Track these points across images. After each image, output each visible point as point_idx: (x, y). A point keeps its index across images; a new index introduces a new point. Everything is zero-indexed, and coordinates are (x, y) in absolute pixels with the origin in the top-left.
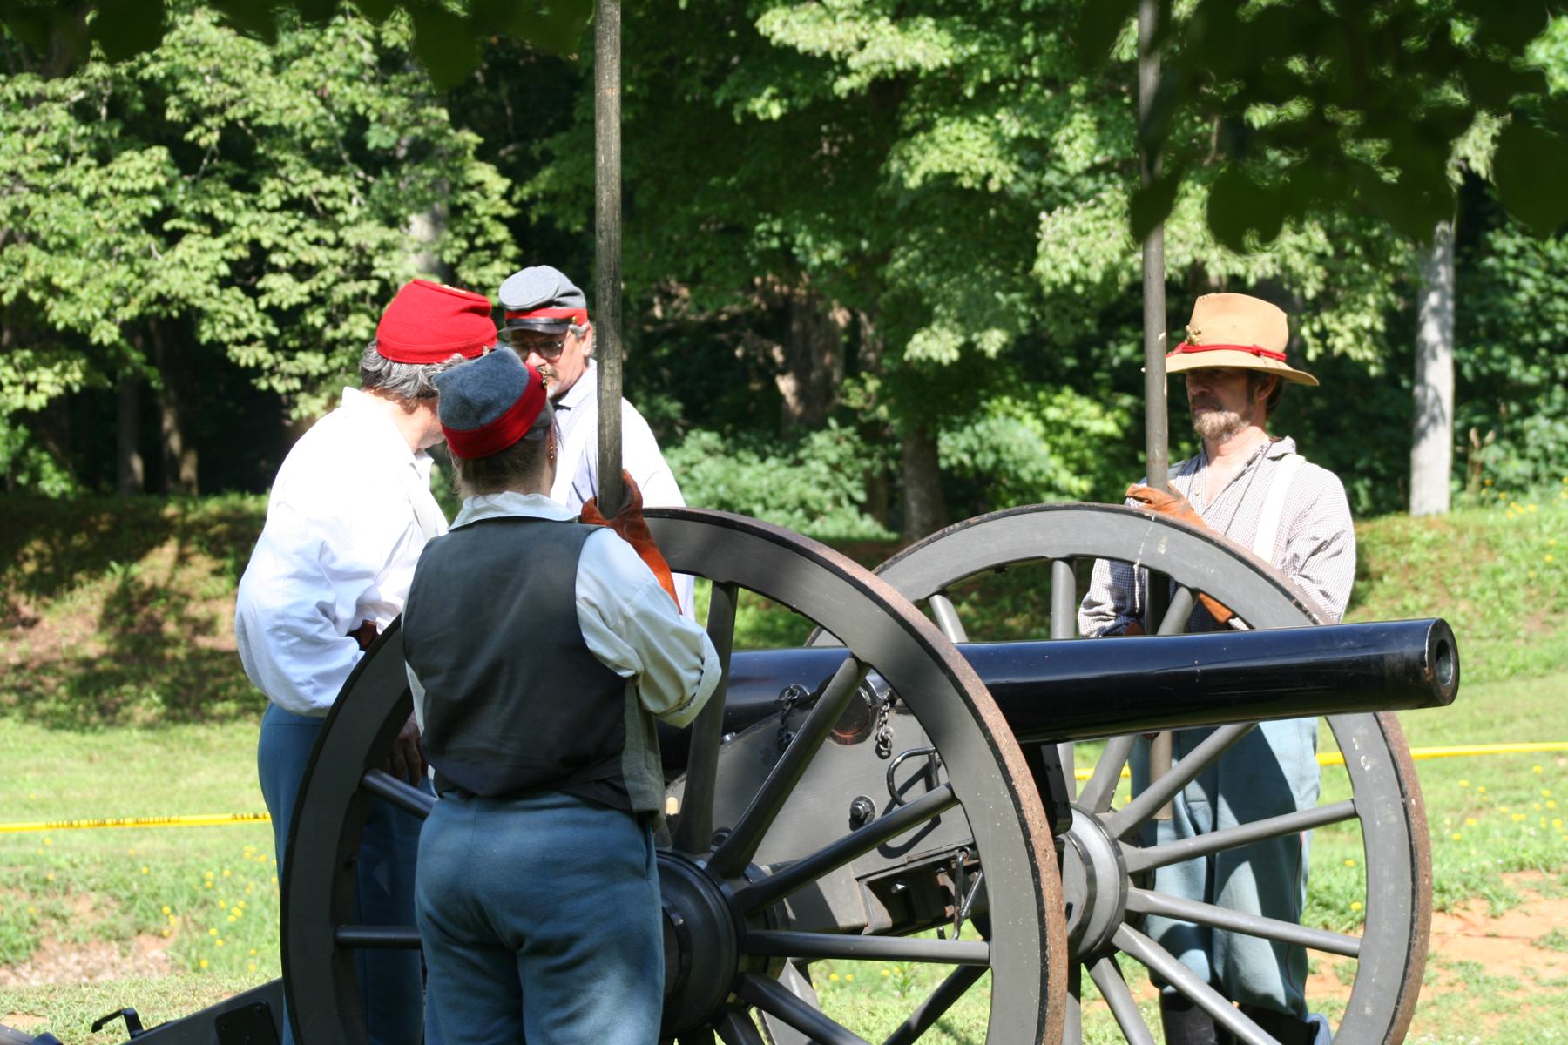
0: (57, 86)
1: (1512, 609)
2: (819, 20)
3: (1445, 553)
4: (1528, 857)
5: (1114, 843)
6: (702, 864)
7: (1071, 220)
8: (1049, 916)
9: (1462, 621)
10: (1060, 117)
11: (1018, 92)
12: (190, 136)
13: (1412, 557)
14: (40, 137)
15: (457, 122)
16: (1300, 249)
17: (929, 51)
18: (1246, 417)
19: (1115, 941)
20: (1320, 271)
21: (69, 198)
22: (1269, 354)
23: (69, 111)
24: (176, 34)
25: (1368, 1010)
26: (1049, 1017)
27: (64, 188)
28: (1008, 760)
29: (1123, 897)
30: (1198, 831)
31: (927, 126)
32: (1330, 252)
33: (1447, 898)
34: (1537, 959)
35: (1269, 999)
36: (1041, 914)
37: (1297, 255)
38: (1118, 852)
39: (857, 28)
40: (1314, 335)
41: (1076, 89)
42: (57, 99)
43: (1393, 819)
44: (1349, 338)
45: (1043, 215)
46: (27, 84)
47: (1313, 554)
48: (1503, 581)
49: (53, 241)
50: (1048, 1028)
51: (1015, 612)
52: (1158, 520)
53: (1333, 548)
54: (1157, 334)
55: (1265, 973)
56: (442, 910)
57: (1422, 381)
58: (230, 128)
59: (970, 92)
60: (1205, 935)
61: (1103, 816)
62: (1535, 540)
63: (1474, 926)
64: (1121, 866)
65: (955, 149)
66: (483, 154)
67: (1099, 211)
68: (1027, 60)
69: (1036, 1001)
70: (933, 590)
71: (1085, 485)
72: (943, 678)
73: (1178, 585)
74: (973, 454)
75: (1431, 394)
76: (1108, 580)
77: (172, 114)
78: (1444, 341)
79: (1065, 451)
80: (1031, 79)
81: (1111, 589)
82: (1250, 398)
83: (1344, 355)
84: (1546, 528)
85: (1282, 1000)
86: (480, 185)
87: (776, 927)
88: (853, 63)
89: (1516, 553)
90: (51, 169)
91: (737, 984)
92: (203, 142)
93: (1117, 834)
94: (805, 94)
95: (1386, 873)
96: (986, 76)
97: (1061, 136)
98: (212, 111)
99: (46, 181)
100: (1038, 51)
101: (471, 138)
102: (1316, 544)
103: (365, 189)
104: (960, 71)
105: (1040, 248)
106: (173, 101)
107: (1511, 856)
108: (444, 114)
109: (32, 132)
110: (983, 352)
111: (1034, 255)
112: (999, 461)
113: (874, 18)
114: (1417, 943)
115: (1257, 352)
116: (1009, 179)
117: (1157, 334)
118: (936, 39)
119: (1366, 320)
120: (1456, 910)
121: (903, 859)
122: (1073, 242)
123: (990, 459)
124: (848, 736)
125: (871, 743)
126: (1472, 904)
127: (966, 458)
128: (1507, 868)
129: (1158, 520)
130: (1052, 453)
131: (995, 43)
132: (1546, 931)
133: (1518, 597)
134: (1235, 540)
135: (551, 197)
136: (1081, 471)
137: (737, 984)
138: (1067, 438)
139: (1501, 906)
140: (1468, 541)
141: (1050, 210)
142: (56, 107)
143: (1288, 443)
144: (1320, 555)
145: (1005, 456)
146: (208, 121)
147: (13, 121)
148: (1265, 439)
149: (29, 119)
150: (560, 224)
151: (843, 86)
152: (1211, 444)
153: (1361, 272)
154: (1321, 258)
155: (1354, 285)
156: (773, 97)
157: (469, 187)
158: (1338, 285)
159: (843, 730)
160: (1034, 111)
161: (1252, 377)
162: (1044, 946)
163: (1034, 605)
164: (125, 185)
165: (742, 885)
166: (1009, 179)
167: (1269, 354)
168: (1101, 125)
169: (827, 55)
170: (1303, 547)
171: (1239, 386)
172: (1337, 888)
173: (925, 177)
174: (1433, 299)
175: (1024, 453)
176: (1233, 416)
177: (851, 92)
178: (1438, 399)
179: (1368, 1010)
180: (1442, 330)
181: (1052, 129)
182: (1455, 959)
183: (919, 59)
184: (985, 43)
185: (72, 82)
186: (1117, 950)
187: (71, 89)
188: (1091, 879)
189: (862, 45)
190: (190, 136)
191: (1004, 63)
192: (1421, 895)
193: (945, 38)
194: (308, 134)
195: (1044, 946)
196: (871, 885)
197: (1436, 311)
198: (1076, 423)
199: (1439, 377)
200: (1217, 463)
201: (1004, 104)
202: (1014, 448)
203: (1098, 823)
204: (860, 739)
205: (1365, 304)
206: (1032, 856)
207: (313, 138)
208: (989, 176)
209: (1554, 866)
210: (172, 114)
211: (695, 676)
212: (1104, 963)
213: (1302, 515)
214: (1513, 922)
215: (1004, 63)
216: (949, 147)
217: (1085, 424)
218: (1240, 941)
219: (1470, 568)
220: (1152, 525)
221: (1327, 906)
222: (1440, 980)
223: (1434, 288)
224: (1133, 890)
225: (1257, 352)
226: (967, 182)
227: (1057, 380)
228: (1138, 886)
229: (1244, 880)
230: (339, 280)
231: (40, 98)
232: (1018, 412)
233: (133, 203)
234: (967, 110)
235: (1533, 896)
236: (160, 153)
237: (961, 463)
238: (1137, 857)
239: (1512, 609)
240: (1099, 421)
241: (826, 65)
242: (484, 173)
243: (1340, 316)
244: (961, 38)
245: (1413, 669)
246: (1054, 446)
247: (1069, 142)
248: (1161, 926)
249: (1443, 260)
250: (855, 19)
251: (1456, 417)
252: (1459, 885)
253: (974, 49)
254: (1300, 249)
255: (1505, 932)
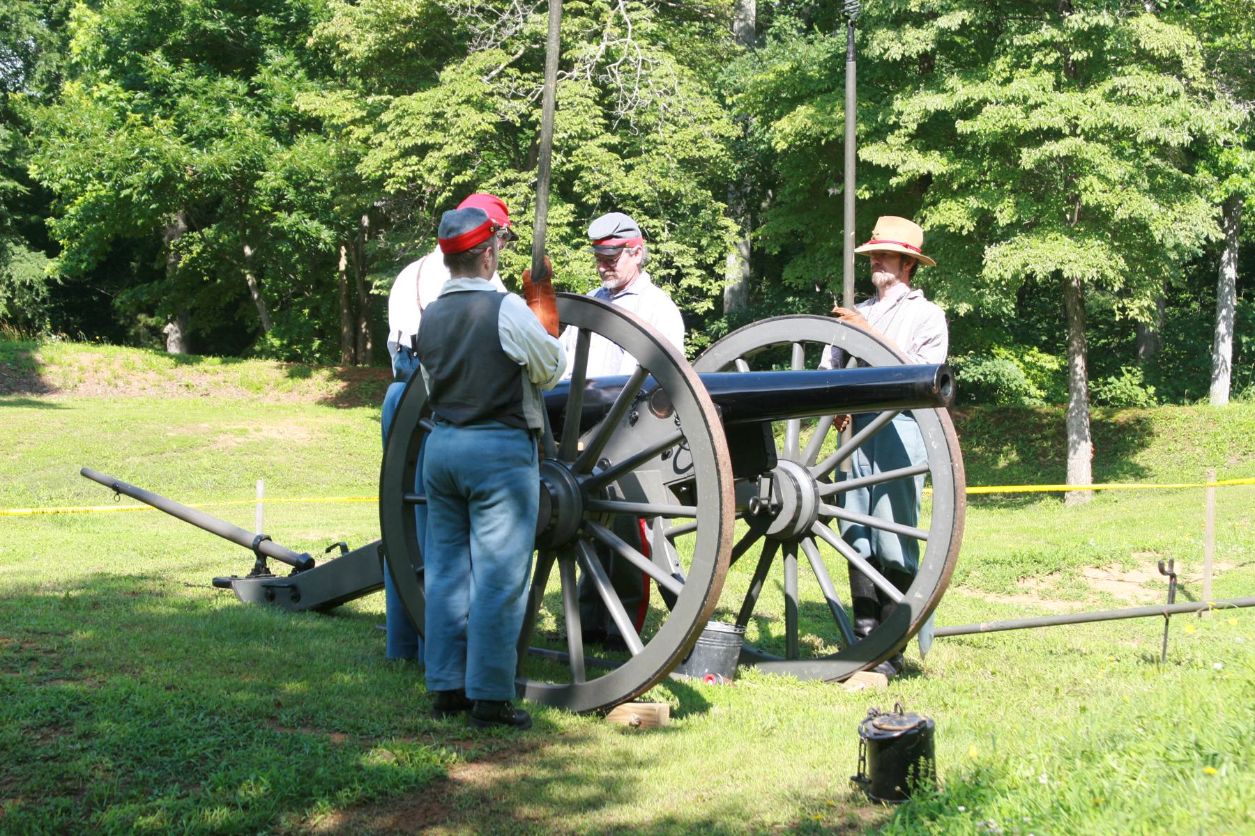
0: (524, 175)
1: (1222, 452)
2: (884, 150)
3: (1191, 424)
4: (1147, 546)
5: (813, 481)
6: (570, 467)
7: (998, 250)
8: (724, 495)
9: (1197, 457)
10: (997, 200)
11: (979, 188)
12: (584, 199)
13: (1174, 426)
14: (515, 198)
15: (716, 197)
16: (1111, 267)
17: (937, 167)
18: (898, 277)
19: (813, 529)
20: (1121, 278)
21: (528, 228)
22: (912, 248)
23: (529, 187)
24: (580, 150)
25: (930, 567)
26: (722, 544)
27: (526, 223)
28: (708, 418)
29: (816, 507)
30: (863, 475)
31: (935, 203)
32: (1127, 269)
33: (1100, 562)
34: (1141, 593)
35: (896, 563)
36: (720, 493)
37: (1110, 270)
38: (815, 486)
39: (902, 154)
40: (1119, 309)
41: (1008, 187)
42: (525, 181)
43: (947, 473)
44: (1137, 311)
45: (986, 247)
46: (511, 174)
47: (925, 344)
48: (1219, 439)
49: (520, 247)
50: (721, 549)
51: (978, 445)
52: (843, 324)
53: (936, 342)
54: (850, 233)
55: (894, 551)
56: (434, 478)
57: (1217, 352)
58: (605, 196)
59: (955, 187)
60: (868, 531)
61: (810, 468)
62: (1237, 419)
63: (1113, 576)
64: (816, 493)
65: (947, 214)
66: (727, 214)
67: (1013, 246)
68: (985, 174)
69: (717, 536)
70: (738, 355)
71: (1043, 394)
72: (680, 376)
73: (850, 356)
74: (985, 376)
75: (1221, 359)
76: (830, 357)
77: (576, 189)
78: (1229, 333)
79: (1034, 378)
80: (986, 182)
81: (831, 361)
82: (901, 269)
83: (1134, 321)
84: (1243, 414)
85: (903, 565)
86: (726, 228)
87: (606, 498)
88: (900, 170)
89: (1227, 426)
90: (521, 214)
91: (583, 525)
92: (590, 202)
93: (815, 477)
94: (881, 188)
95: (942, 499)
96: (963, 181)
97: (998, 208)
98: (597, 187)
99: (516, 219)
100: (989, 169)
101: (722, 205)
102: (925, 340)
103: (672, 229)
104: (952, 176)
105: (983, 263)
106: (577, 182)
107: (1140, 545)
108: (710, 193)
109: (512, 196)
110: (958, 313)
111: (981, 267)
112: (998, 379)
113: (910, 149)
114: (955, 534)
115: (906, 246)
116: (972, 229)
117: (850, 233)
118: (940, 161)
119: (1145, 303)
120: (1105, 568)
121: (685, 475)
122: (999, 260)
123: (994, 379)
124: (663, 414)
125: (673, 418)
126: (1114, 565)
127: (982, 378)
128: (1135, 550)
129: (843, 324)
130: (1026, 378)
131: (970, 164)
132: (1149, 580)
133: (1225, 447)
134: (887, 339)
135: (765, 238)
136: (1040, 388)
137: (583, 525)
138: (1034, 372)
139: (1128, 567)
140: (1203, 418)
141: (990, 243)
142: (523, 184)
143: (920, 292)
144: (928, 345)
145: (1004, 379)
146: (593, 193)
147: (503, 191)
148: (907, 289)
149: (510, 190)
150: (767, 251)
151: (894, 181)
152: (881, 290)
153: (1145, 280)
154: (1122, 272)
155: (1140, 286)
156: (866, 189)
157: (722, 229)
158: (1131, 287)
159: (660, 411)
160: (985, 197)
161: (903, 257)
162: (721, 509)
163: (987, 442)
164: (553, 222)
165: (590, 476)
166: (972, 229)
167: (912, 248)
168: (1017, 204)
169: (887, 166)
170: (919, 341)
171: (896, 262)
172: (1045, 554)
173: (932, 226)
174: (1224, 312)
175: (1012, 377)
176: (891, 276)
177: (898, 184)
178: (1224, 361)
179: (930, 567)
180: (1227, 328)
181: (993, 205)
182: (1100, 589)
183: (931, 169)
184: (964, 163)
185: (532, 173)
186: (815, 535)
187: (531, 176)
188: (799, 498)
189: (904, 162)
190: (584, 199)
191: (972, 173)
192: (958, 511)
193: (945, 160)
194: (643, 199)
195: (721, 509)
196: (671, 487)
197: (1224, 318)
198: (1038, 364)
199: (1225, 350)
200: (882, 301)
201: (972, 194)
202: (1006, 374)
203: (807, 472)
204: (668, 416)
205: (1146, 295)
206: (717, 464)
207: (646, 201)
208: (962, 227)
209: (1161, 551)
210: (576, 189)
211: (552, 368)
212: (807, 540)
213: (921, 326)
214: (1133, 575)
215: (972, 173)
216: (945, 213)
217: (1044, 364)
218: (883, 534)
219: (1203, 432)
220: (840, 326)
221: (1039, 562)
222: (1090, 600)
223: (1226, 306)
224: (822, 504)
225: (906, 246)
226: (952, 230)
227: (1034, 342)
228: (825, 503)
229: (885, 503)
230: (657, 269)
231: (516, 180)
232: (1011, 357)
233: (556, 230)
234: (954, 195)
235: (1147, 564)
236: (571, 207)
237: (979, 379)
238: (825, 489)
239: (1222, 452)
240: (1051, 363)
241: (891, 172)
242: (729, 222)
243: (1132, 301)
244: (951, 161)
245: (928, 387)
246: (1029, 374)
247: (1001, 212)
248: (847, 525)
249: (1230, 292)
250: (901, 150)
251: (1234, 372)
252: (1108, 556)
253: (959, 166)
254: (1111, 267)
255: (1126, 579)
